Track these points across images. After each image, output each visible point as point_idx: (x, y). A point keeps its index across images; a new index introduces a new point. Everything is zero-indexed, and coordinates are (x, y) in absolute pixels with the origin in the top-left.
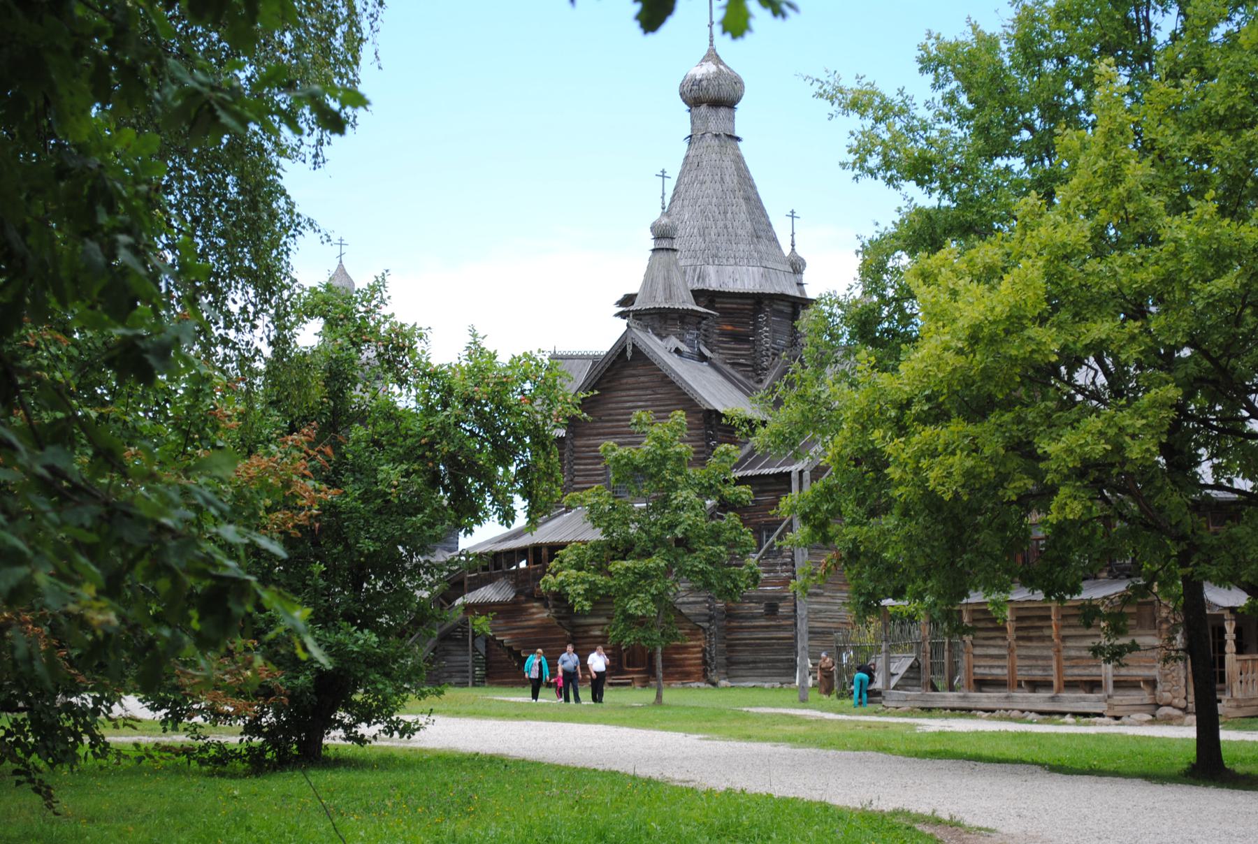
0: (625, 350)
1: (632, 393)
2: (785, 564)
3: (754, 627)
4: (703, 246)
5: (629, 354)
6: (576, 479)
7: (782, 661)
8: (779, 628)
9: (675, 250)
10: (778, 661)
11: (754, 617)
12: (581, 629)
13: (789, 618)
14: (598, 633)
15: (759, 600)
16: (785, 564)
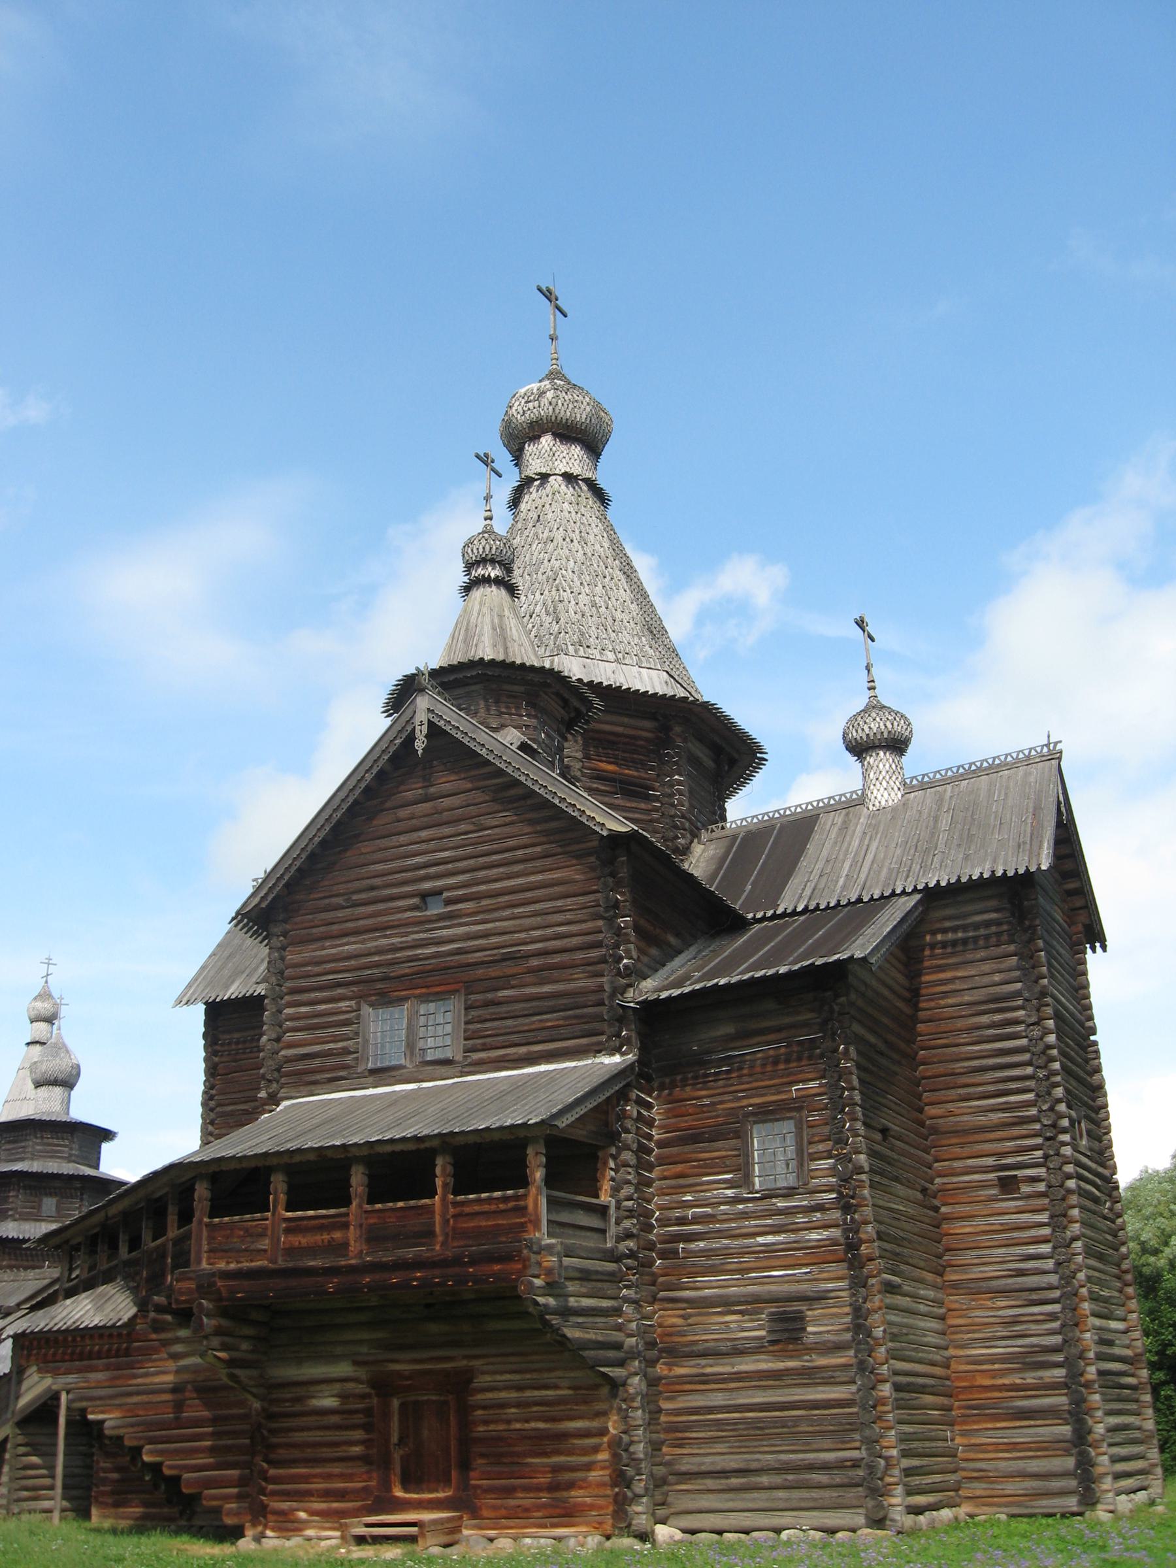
0: (411, 738)
1: (424, 834)
2: (820, 1208)
3: (739, 1377)
4: (555, 628)
5: (420, 745)
6: (288, 1037)
7: (825, 1467)
8: (809, 1376)
9: (512, 590)
10: (811, 1467)
11: (739, 1352)
12: (287, 1394)
13: (838, 1347)
14: (329, 1402)
15: (750, 1305)
16: (820, 1208)
